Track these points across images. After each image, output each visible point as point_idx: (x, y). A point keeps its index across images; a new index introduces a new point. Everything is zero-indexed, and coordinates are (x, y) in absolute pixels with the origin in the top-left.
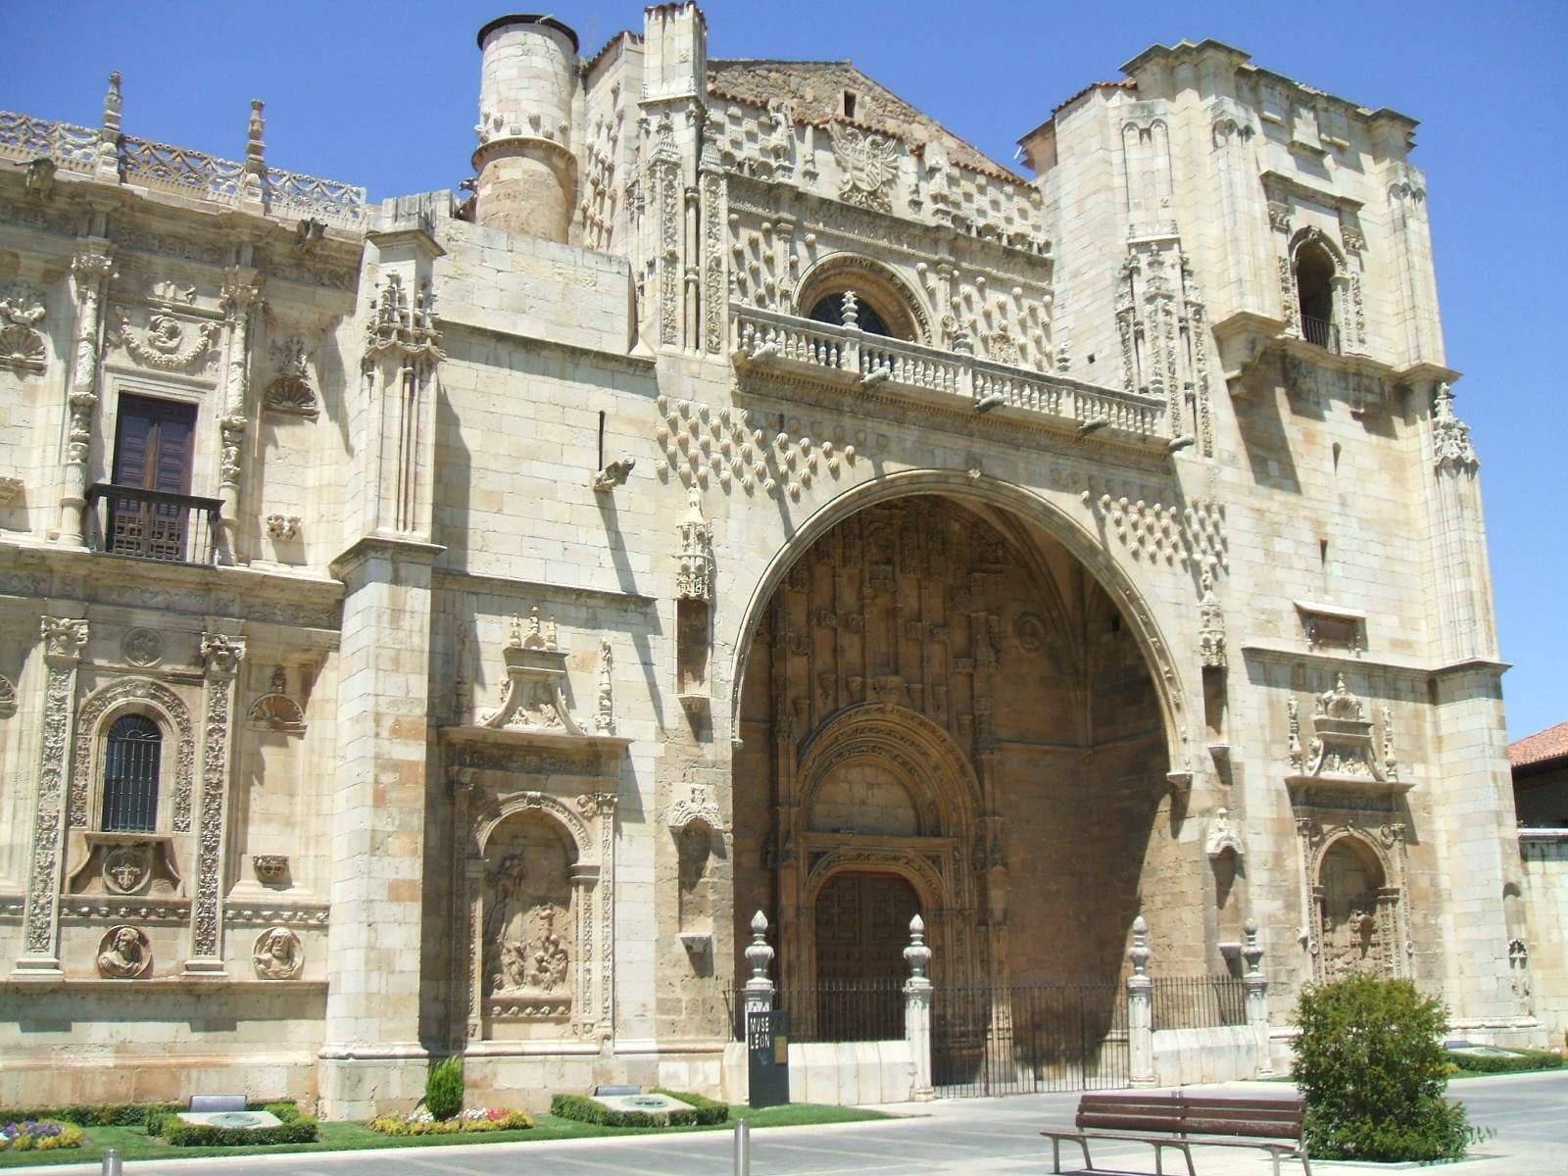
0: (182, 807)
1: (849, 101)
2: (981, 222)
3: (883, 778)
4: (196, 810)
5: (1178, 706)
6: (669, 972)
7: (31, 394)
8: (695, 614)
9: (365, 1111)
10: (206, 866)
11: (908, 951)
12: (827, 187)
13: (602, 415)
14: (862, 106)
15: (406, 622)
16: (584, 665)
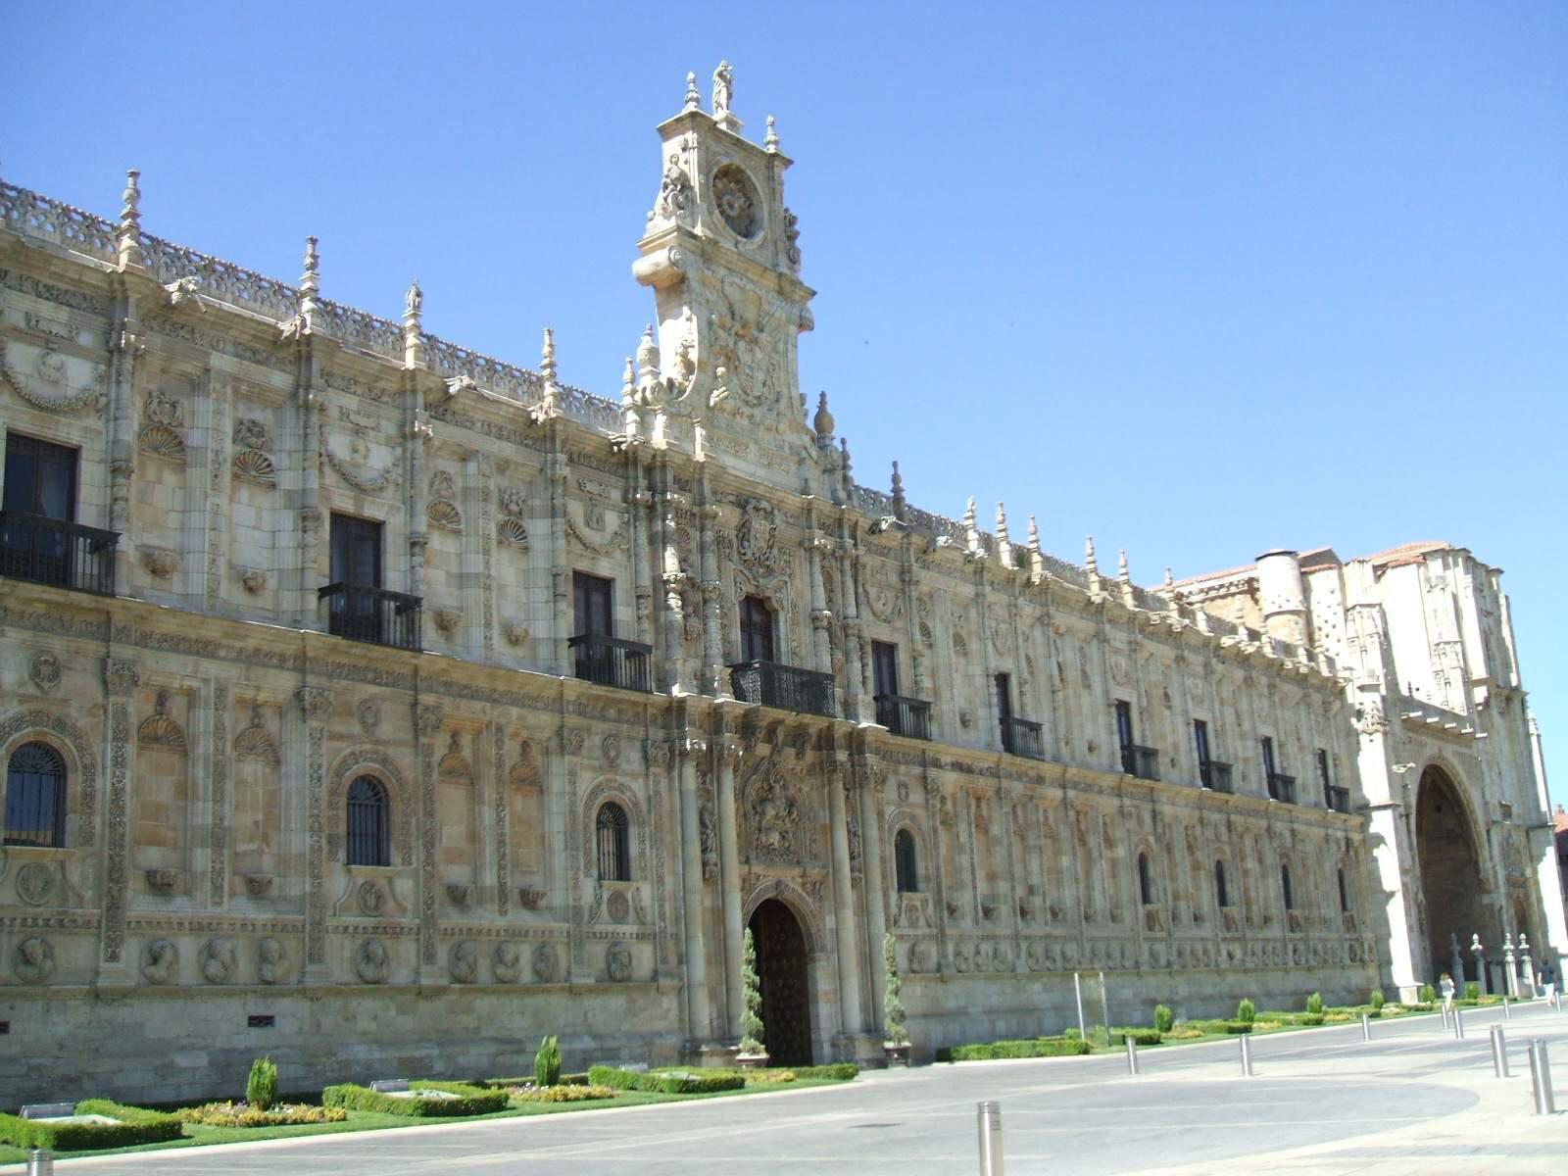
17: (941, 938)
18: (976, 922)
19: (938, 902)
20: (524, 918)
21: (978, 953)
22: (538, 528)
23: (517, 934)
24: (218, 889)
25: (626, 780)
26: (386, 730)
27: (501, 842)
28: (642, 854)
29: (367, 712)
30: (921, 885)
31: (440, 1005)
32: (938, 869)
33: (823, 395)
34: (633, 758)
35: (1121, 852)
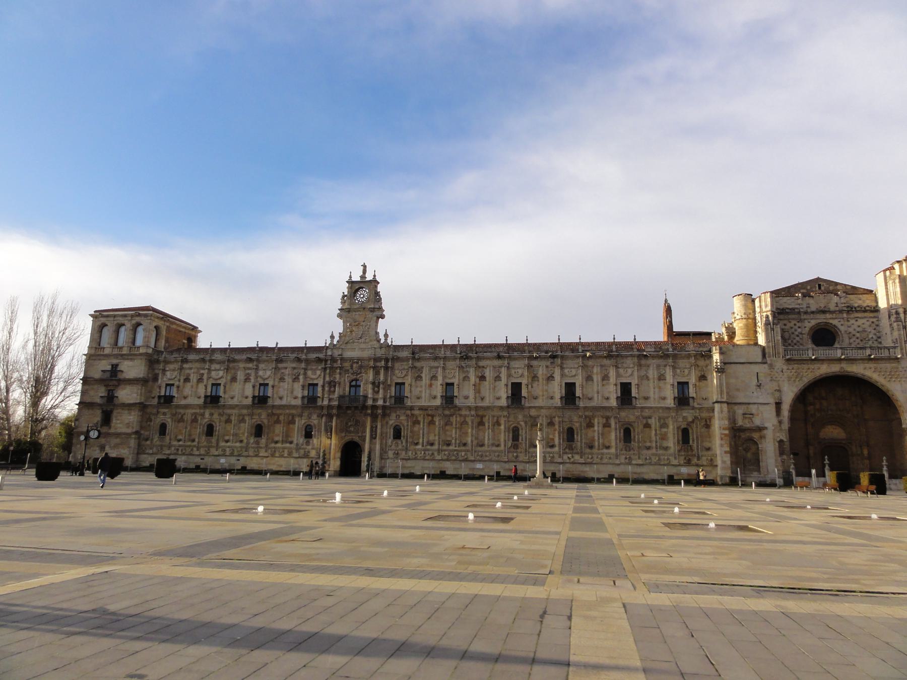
0: (693, 441)
1: (820, 286)
2: (856, 305)
3: (837, 427)
4: (695, 441)
5: (903, 412)
6: (778, 464)
7: (665, 383)
8: (778, 405)
9: (723, 482)
10: (698, 449)
11: (825, 462)
12: (813, 308)
13: (757, 373)
14: (823, 285)
15: (723, 413)
16: (758, 415)
17: (407, 449)
18: (423, 446)
19: (407, 441)
20: (288, 445)
21: (421, 453)
22: (301, 377)
23: (284, 448)
24: (233, 442)
25: (313, 421)
26: (263, 417)
27: (283, 433)
28: (315, 434)
29: (260, 415)
30: (402, 438)
31: (269, 458)
32: (407, 434)
33: (386, 330)
34: (315, 417)
35: (502, 427)
